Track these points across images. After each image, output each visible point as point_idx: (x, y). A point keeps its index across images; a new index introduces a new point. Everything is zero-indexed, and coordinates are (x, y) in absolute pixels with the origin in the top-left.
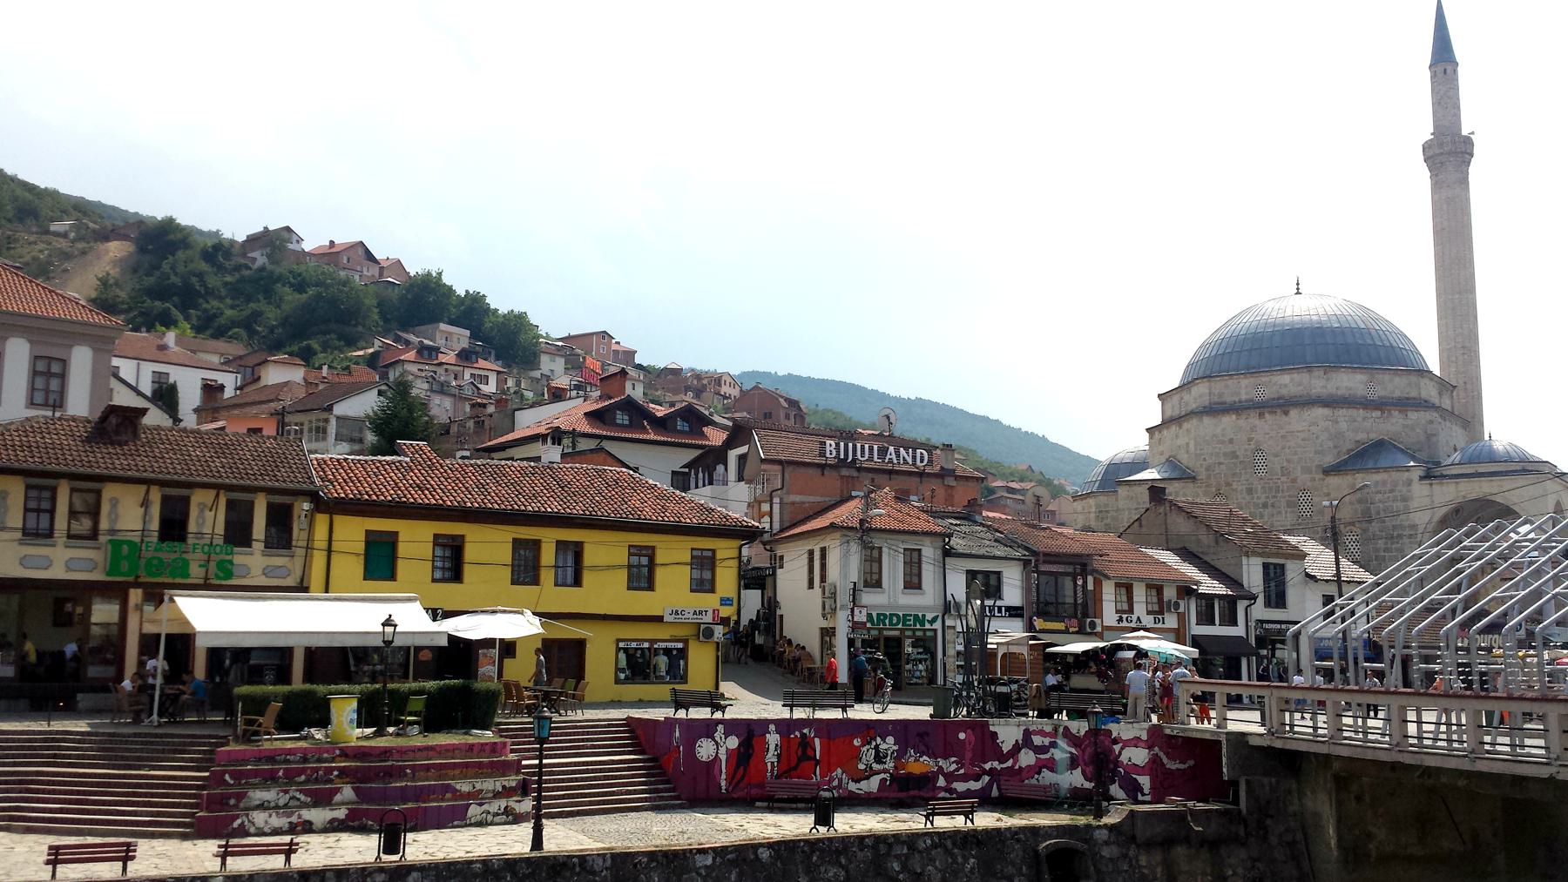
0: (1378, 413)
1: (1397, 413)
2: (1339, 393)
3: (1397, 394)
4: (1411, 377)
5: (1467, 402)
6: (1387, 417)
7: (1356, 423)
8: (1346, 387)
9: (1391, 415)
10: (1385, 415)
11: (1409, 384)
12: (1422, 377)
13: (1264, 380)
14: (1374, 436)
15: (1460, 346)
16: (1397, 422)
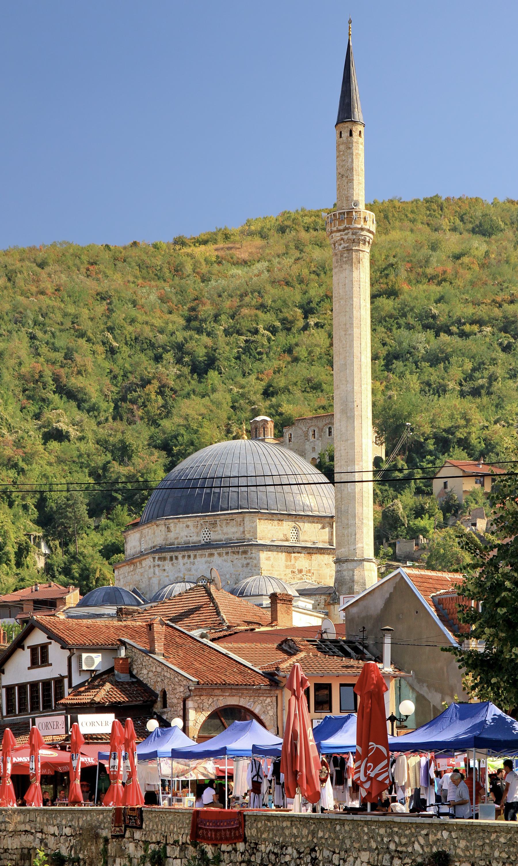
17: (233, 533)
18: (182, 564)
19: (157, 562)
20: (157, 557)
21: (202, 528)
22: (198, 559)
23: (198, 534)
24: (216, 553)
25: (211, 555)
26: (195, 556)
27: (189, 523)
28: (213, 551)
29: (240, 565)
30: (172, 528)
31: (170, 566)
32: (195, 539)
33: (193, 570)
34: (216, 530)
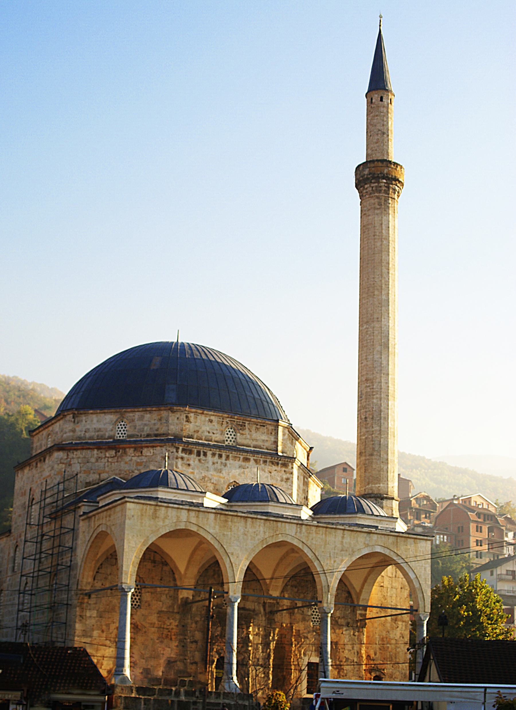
0: (113, 453)
1: (132, 450)
2: (87, 435)
3: (147, 430)
4: (162, 412)
5: (366, 438)
6: (121, 456)
7: (89, 465)
8: (95, 429)
9: (125, 453)
10: (119, 454)
11: (160, 420)
12: (173, 412)
13: (50, 428)
14: (104, 476)
15: (364, 380)
16: (131, 460)
17: (263, 441)
18: (211, 463)
19: (180, 454)
20: (181, 448)
21: (227, 426)
22: (231, 461)
23: (222, 433)
24: (252, 458)
25: (247, 460)
26: (228, 457)
27: (212, 418)
28: (249, 456)
29: (279, 479)
30: (192, 419)
31: (197, 461)
32: (217, 437)
33: (224, 472)
34: (243, 432)
